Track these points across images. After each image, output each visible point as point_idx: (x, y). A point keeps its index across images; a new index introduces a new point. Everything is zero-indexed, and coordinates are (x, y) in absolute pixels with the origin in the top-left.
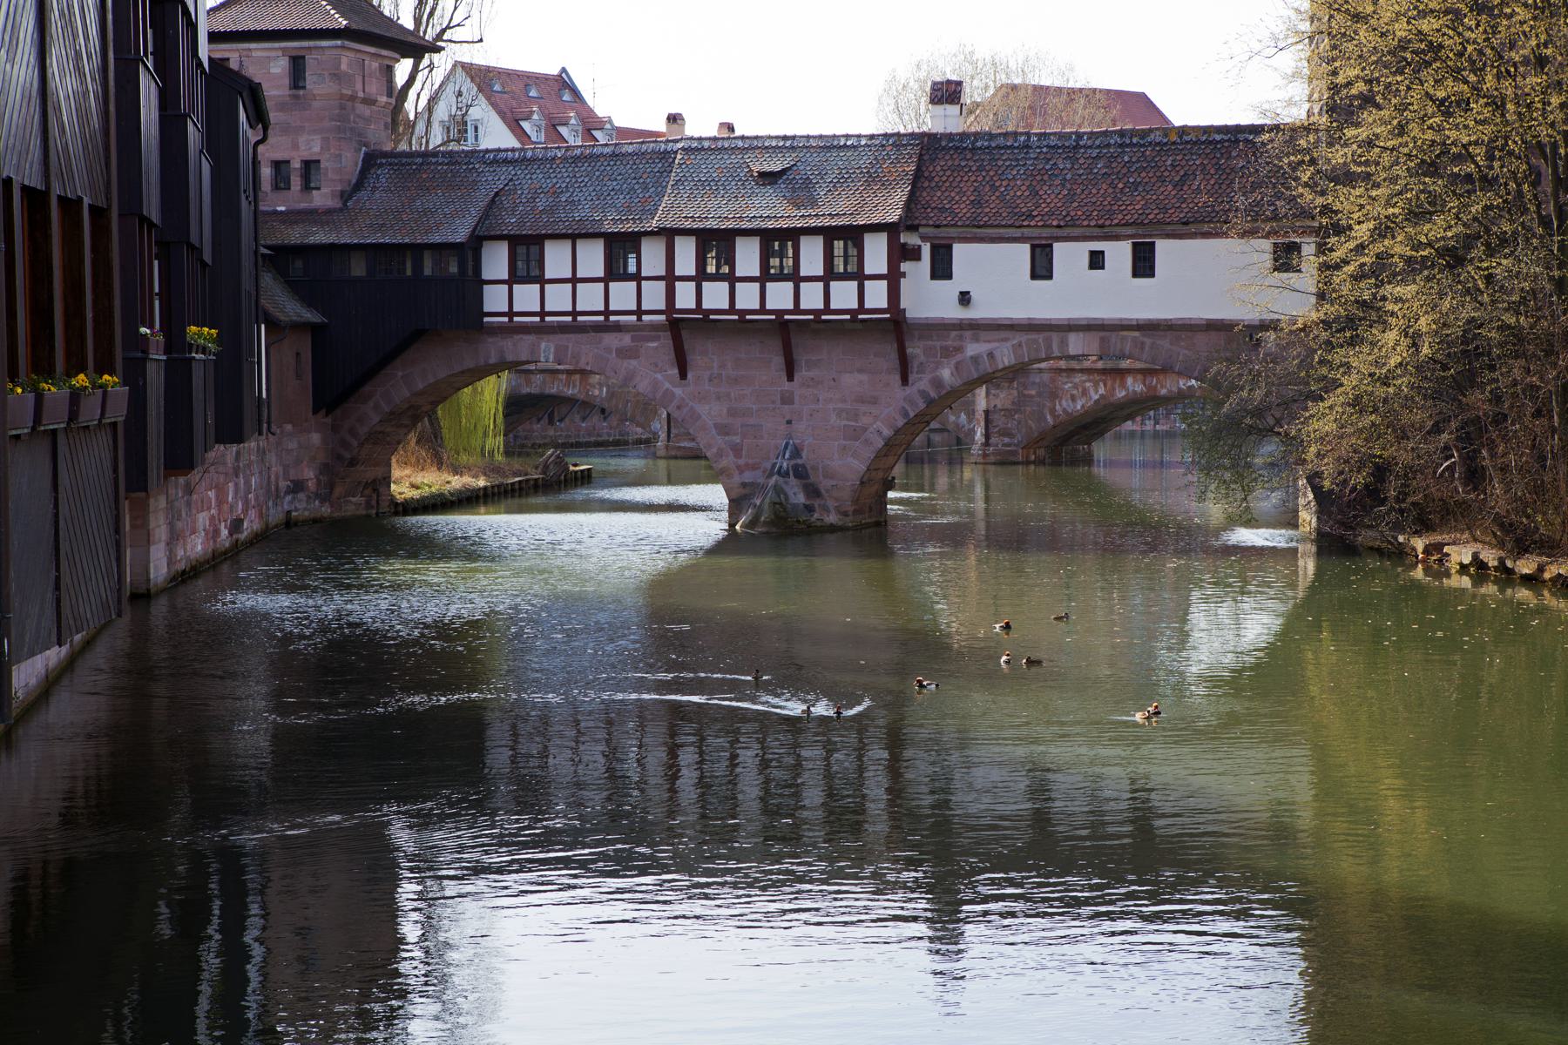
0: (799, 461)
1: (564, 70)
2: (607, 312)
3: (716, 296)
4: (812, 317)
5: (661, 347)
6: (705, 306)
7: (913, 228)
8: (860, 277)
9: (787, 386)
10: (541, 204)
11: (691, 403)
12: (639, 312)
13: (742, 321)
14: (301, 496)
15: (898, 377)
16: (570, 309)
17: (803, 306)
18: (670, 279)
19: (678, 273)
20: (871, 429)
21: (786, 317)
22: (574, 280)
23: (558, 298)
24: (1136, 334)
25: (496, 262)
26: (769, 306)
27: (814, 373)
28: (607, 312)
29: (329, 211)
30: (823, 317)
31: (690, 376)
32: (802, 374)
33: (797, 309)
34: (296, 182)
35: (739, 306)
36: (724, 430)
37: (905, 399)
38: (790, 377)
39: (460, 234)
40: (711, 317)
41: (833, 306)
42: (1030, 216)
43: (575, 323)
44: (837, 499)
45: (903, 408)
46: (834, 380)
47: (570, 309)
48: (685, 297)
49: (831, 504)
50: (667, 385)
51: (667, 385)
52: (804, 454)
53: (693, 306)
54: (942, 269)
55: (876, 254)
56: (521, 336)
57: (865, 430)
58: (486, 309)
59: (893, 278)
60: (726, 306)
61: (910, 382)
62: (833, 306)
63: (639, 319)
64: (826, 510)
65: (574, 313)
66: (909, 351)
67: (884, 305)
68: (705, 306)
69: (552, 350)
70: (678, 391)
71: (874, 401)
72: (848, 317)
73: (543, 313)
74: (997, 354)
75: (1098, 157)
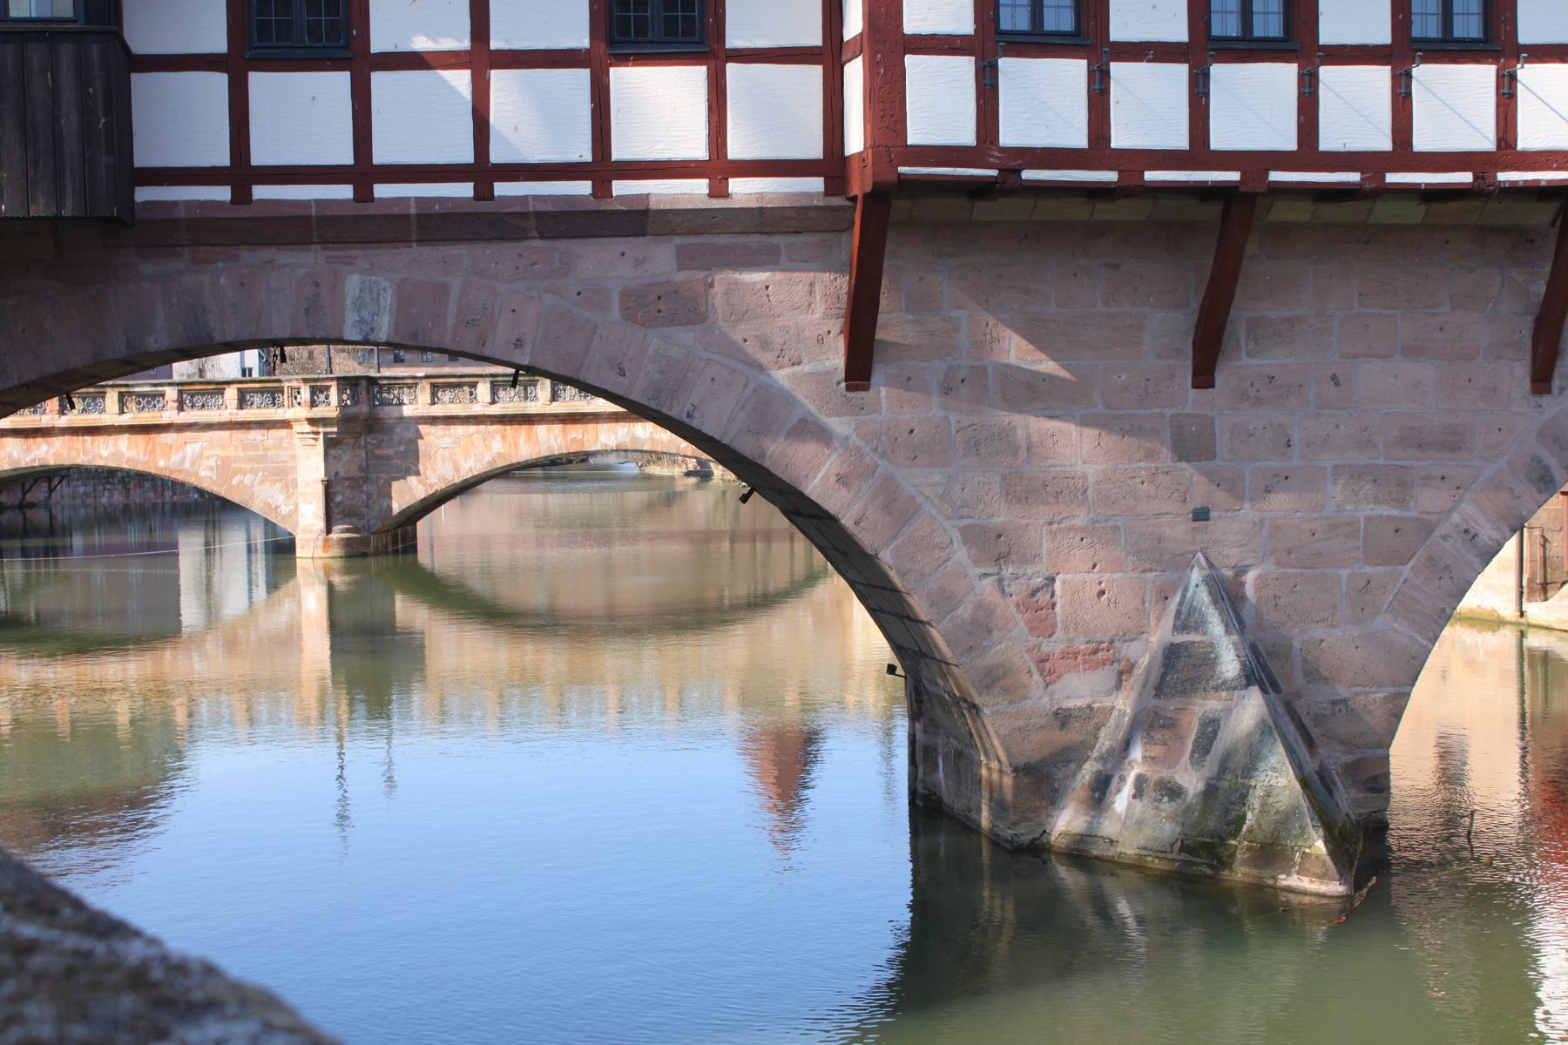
4: (1354, 177)
6: (1009, 136)
9: (1192, 400)
11: (884, 466)
13: (1131, 190)
15: (1520, 371)
16: (466, 155)
17: (1328, 142)
20: (1443, 530)
21: (1276, 176)
26: (1217, 142)
27: (1275, 360)
28: (602, 168)
30: (1392, 178)
33: (1308, 152)
35: (1120, 139)
37: (1540, 434)
38: (1203, 376)
40: (1027, 175)
41: (1422, 142)
43: (484, 207)
44: (1347, 744)
45: (1537, 460)
46: (1334, 378)
47: (466, 155)
53: (966, 135)
56: (267, 253)
57: (1427, 528)
58: (144, 157)
61: (1556, 383)
62: (1422, 142)
63: (719, 191)
68: (1009, 136)
69: (388, 299)
71: (1452, 442)
72: (1465, 177)
73: (363, 172)
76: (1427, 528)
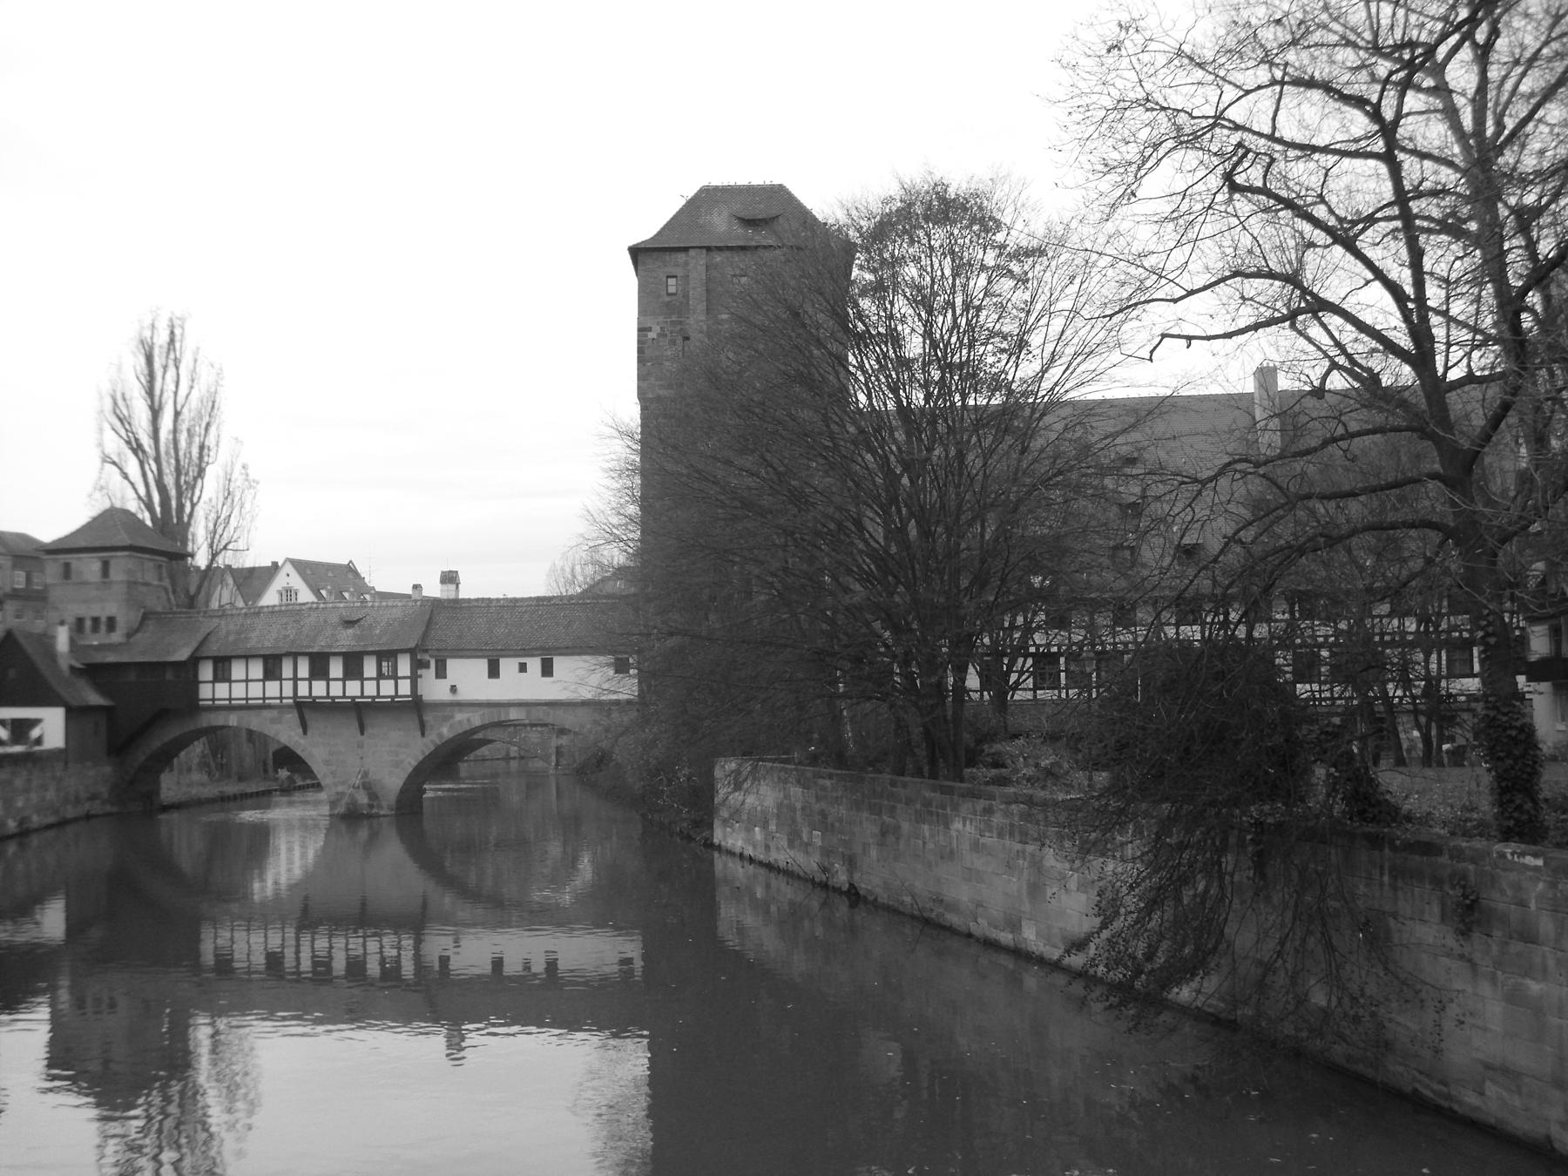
0: (367, 780)
1: (351, 562)
2: (264, 698)
3: (319, 688)
5: (293, 717)
7: (426, 651)
8: (396, 678)
9: (360, 738)
10: (231, 638)
12: (281, 698)
13: (334, 702)
14: (97, 802)
15: (419, 733)
17: (365, 694)
18: (295, 679)
19: (299, 676)
22: (247, 681)
23: (238, 691)
24: (545, 708)
25: (206, 671)
28: (264, 698)
29: (120, 644)
31: (309, 733)
32: (368, 731)
33: (362, 696)
34: (103, 628)
35: (331, 695)
36: (327, 763)
38: (362, 733)
39: (183, 655)
42: (486, 644)
48: (303, 690)
49: (384, 804)
50: (297, 738)
51: (297, 738)
52: (370, 776)
54: (441, 673)
55: (404, 667)
57: (402, 762)
59: (414, 679)
60: (325, 694)
64: (380, 807)
65: (247, 699)
66: (426, 718)
67: (409, 693)
70: (302, 741)
73: (230, 699)
74: (472, 719)
75: (526, 612)
76: (402, 762)
